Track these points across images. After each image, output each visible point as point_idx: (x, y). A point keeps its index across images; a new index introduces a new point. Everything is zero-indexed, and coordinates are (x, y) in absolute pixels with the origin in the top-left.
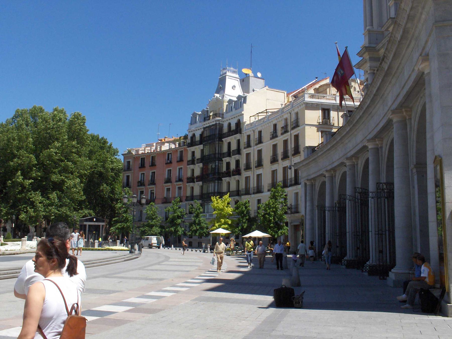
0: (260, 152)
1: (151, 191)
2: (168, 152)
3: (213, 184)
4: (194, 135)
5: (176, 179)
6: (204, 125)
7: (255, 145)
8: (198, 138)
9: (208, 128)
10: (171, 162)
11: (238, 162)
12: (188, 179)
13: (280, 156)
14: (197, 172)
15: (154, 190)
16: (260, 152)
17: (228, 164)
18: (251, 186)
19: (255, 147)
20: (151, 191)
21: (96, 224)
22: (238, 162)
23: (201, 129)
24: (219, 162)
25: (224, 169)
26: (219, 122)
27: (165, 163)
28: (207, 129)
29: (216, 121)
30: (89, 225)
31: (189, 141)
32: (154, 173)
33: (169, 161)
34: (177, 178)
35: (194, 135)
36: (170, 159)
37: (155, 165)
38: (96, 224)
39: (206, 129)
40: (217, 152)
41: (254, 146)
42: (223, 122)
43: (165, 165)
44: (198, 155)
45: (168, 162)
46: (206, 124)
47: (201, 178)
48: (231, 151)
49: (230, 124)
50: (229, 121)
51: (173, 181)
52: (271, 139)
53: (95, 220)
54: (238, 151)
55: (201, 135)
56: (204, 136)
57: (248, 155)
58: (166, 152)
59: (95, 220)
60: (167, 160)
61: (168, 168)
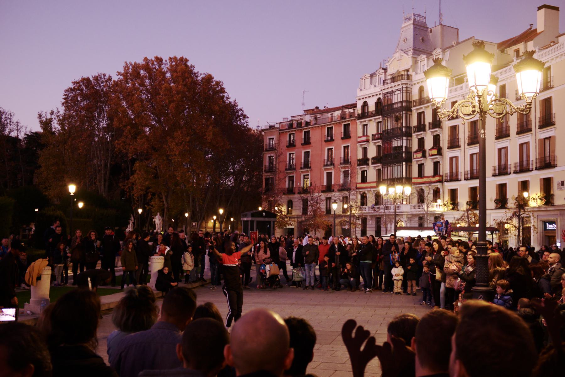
1: (304, 176)
3: (399, 167)
4: (365, 104)
5: (341, 160)
6: (384, 89)
8: (372, 108)
10: (332, 140)
11: (437, 139)
13: (513, 129)
14: (372, 153)
15: (308, 175)
18: (461, 170)
20: (304, 176)
21: (267, 219)
22: (437, 139)
26: (407, 85)
27: (323, 140)
29: (402, 84)
30: (257, 221)
31: (359, 110)
32: (307, 154)
33: (329, 138)
34: (342, 159)
37: (310, 143)
38: (267, 219)
42: (412, 85)
43: (324, 143)
45: (328, 138)
47: (376, 160)
51: (335, 164)
53: (264, 214)
55: (378, 103)
59: (264, 214)
60: (326, 136)
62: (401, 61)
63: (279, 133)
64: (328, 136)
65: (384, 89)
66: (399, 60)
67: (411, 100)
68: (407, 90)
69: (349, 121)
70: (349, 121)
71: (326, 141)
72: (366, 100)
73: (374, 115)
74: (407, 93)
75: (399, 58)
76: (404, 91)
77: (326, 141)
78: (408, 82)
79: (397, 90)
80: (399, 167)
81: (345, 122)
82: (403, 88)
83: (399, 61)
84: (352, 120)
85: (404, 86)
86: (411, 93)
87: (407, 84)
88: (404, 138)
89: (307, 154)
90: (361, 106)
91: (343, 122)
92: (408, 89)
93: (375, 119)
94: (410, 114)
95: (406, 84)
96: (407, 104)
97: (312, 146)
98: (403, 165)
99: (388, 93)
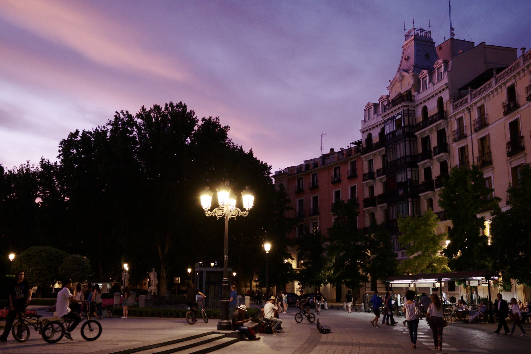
0: (484, 142)
2: (334, 165)
4: (369, 138)
7: (473, 131)
8: (376, 139)
9: (390, 120)
10: (339, 181)
12: (365, 200)
14: (379, 190)
16: (484, 142)
17: (428, 171)
19: (474, 135)
23: (380, 124)
24: (411, 169)
25: (422, 179)
26: (408, 107)
28: (390, 121)
29: (402, 107)
32: (315, 198)
33: (336, 179)
35: (370, 135)
36: (338, 176)
40: (408, 153)
41: (471, 134)
44: (378, 165)
45: (335, 179)
46: (388, 114)
48: (432, 149)
49: (425, 109)
50: (423, 105)
52: (505, 114)
54: (443, 147)
56: (385, 134)
57: (463, 151)
63: (288, 179)
67: (414, 124)
68: (408, 113)
69: (354, 158)
70: (354, 158)
72: (369, 132)
73: (379, 145)
74: (409, 116)
76: (405, 115)
77: (334, 183)
78: (410, 104)
79: (398, 114)
80: (404, 204)
81: (351, 159)
82: (403, 111)
83: (400, 83)
86: (415, 116)
87: (409, 106)
88: (408, 169)
89: (315, 198)
90: (366, 139)
91: (349, 160)
92: (410, 112)
93: (379, 152)
94: (413, 141)
95: (406, 106)
96: (409, 129)
97: (320, 190)
98: (408, 202)
99: (389, 119)
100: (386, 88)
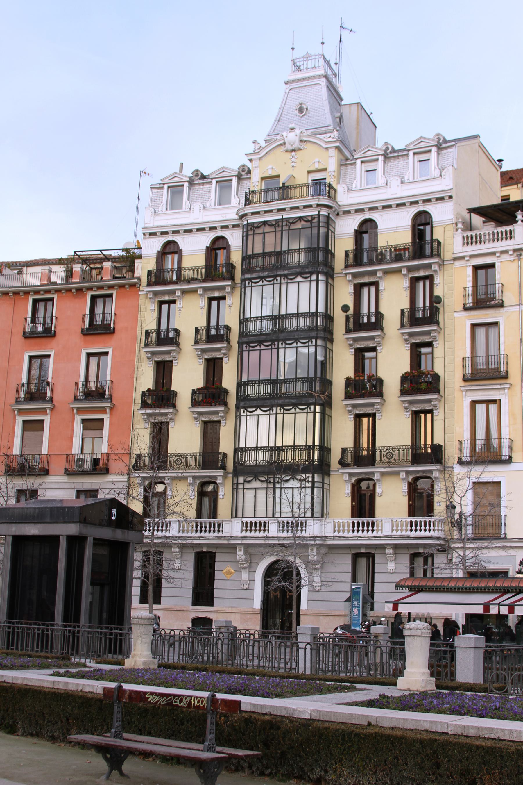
9: (271, 226)
28: (267, 229)
29: (318, 205)
33: (40, 328)
39: (258, 231)
42: (338, 214)
43: (18, 338)
58: (27, 293)
60: (29, 320)
61: (32, 350)
62: (299, 154)
64: (34, 320)
65: (253, 214)
66: (293, 150)
70: (111, 287)
71: (27, 336)
75: (297, 145)
76: (321, 224)
79: (300, 218)
82: (319, 215)
83: (293, 153)
84: (122, 286)
85: (324, 212)
90: (158, 252)
93: (205, 289)
99: (265, 223)
100: (246, 154)
